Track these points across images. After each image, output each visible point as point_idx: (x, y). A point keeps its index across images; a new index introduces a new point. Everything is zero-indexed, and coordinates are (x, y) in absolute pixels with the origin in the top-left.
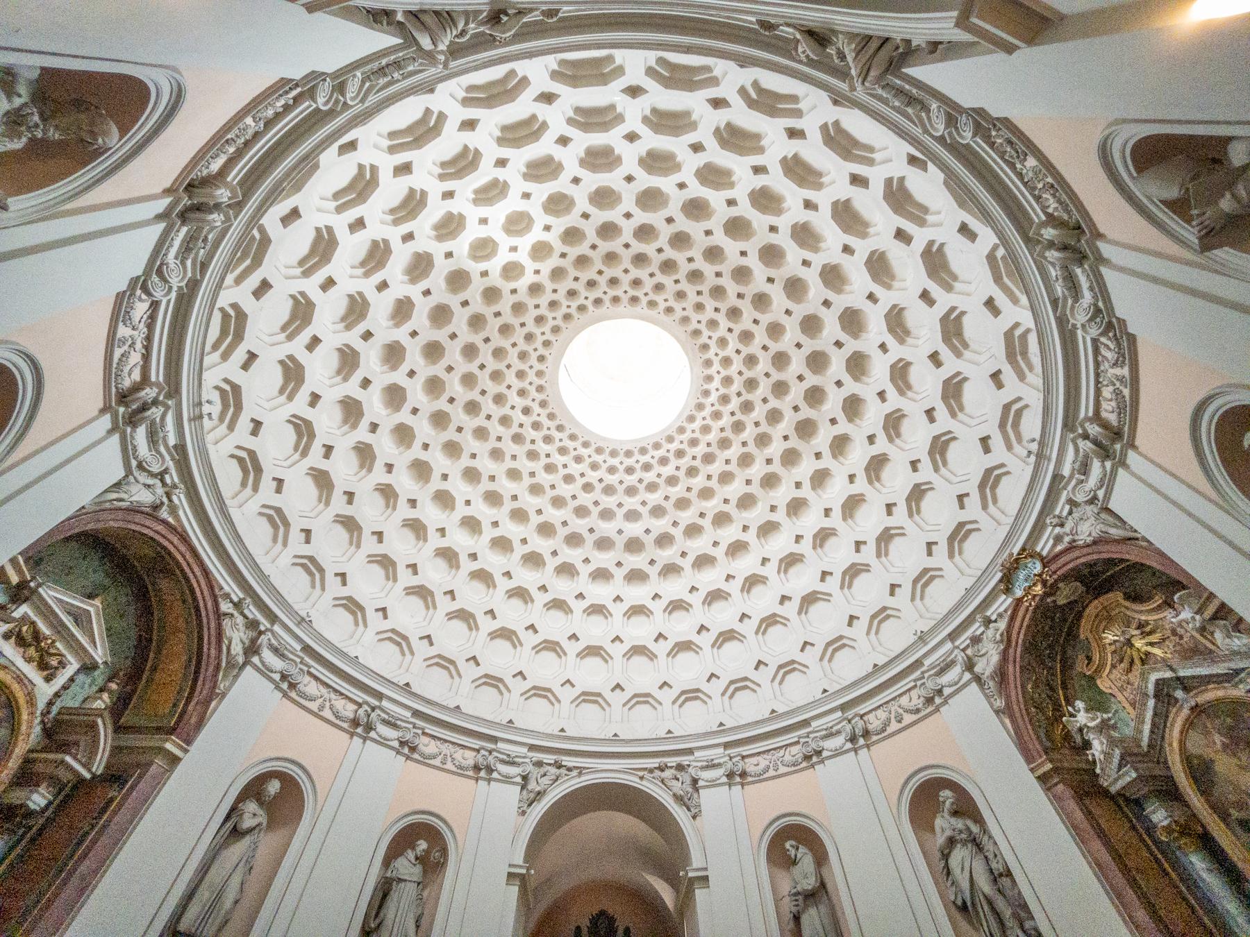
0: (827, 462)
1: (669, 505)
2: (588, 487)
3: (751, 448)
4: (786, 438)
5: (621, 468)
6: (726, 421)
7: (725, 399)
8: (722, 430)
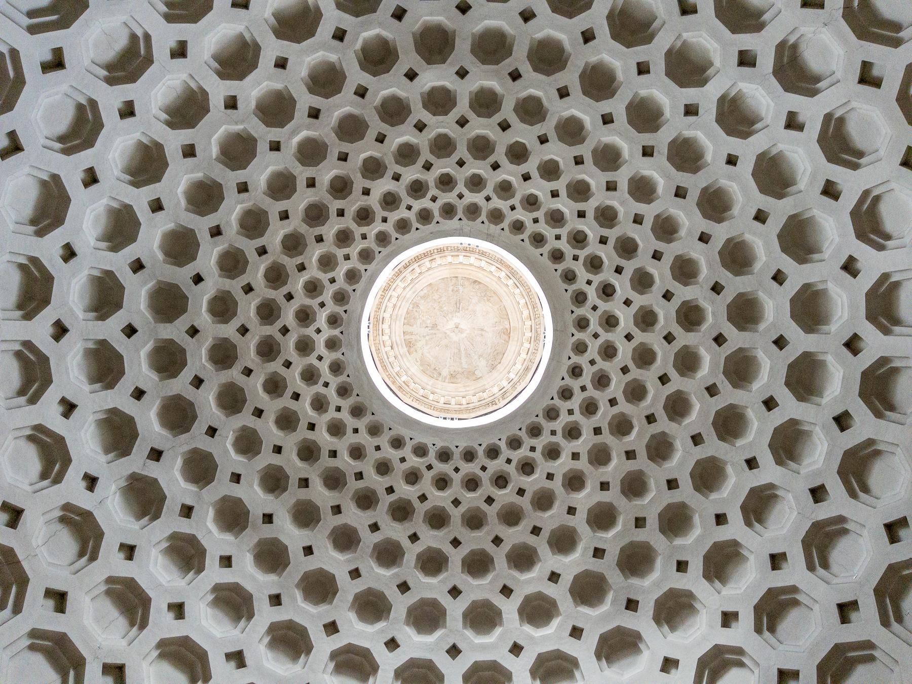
0: (118, 262)
1: (376, 125)
2: (518, 154)
3: (249, 247)
4: (198, 279)
5: (461, 188)
6: (298, 284)
7: (305, 316)
8: (302, 268)
